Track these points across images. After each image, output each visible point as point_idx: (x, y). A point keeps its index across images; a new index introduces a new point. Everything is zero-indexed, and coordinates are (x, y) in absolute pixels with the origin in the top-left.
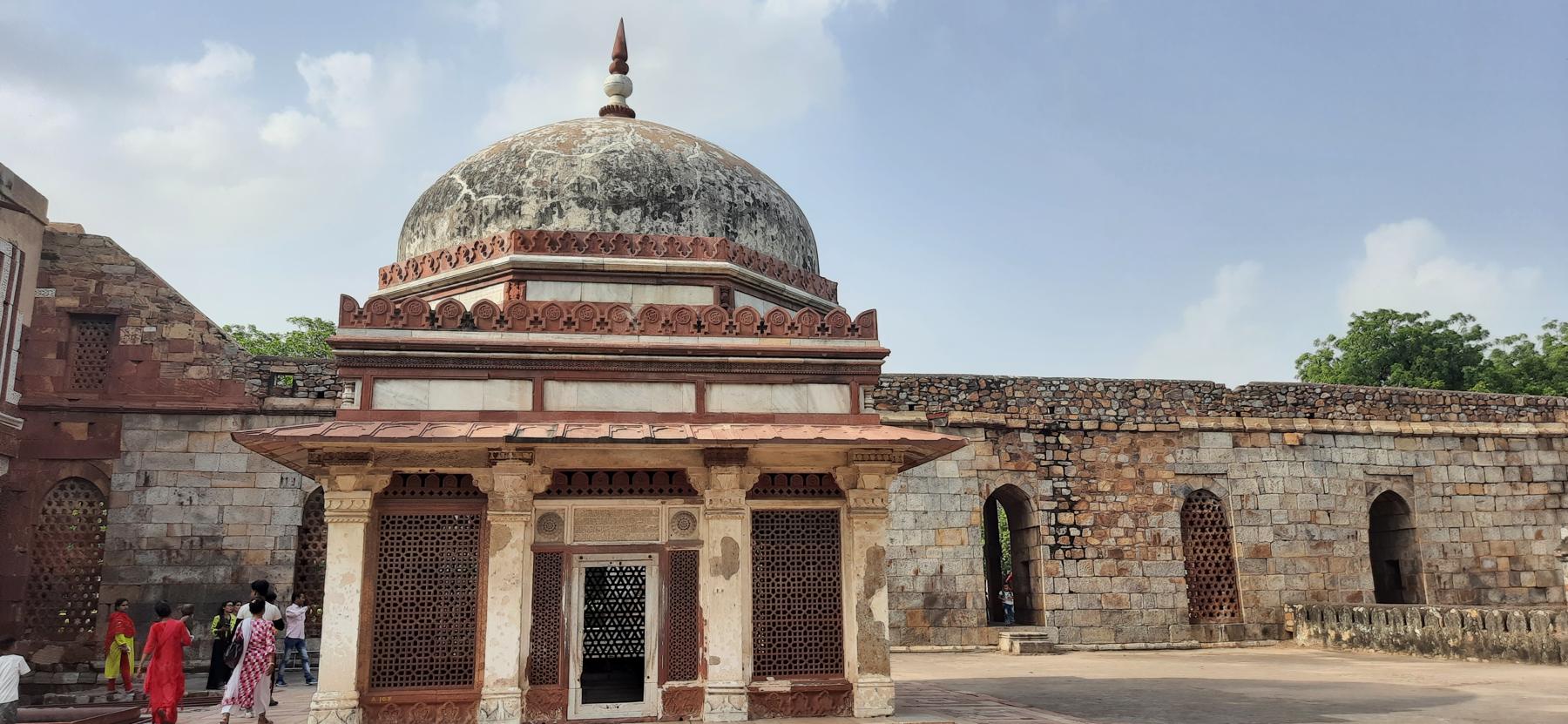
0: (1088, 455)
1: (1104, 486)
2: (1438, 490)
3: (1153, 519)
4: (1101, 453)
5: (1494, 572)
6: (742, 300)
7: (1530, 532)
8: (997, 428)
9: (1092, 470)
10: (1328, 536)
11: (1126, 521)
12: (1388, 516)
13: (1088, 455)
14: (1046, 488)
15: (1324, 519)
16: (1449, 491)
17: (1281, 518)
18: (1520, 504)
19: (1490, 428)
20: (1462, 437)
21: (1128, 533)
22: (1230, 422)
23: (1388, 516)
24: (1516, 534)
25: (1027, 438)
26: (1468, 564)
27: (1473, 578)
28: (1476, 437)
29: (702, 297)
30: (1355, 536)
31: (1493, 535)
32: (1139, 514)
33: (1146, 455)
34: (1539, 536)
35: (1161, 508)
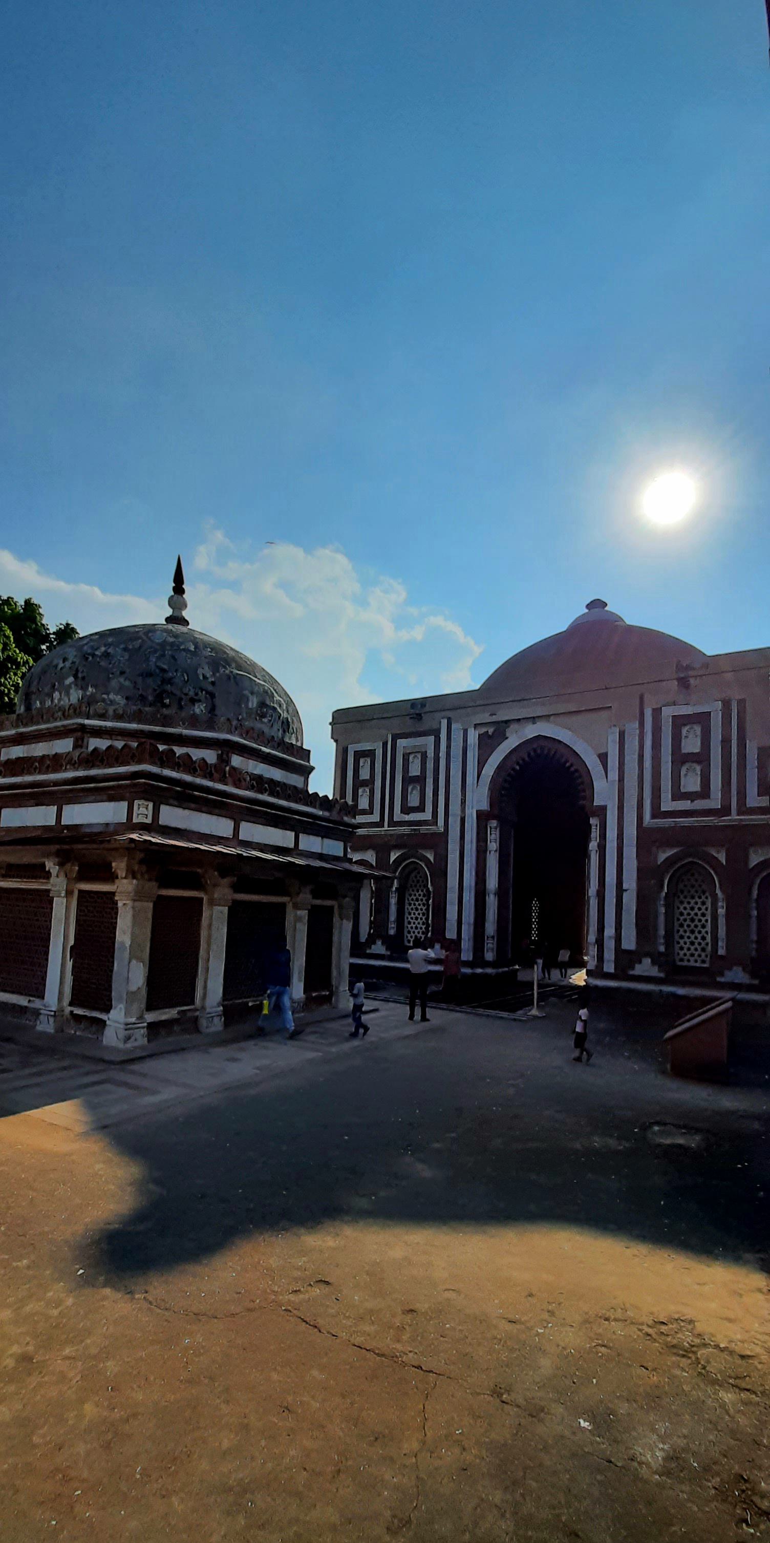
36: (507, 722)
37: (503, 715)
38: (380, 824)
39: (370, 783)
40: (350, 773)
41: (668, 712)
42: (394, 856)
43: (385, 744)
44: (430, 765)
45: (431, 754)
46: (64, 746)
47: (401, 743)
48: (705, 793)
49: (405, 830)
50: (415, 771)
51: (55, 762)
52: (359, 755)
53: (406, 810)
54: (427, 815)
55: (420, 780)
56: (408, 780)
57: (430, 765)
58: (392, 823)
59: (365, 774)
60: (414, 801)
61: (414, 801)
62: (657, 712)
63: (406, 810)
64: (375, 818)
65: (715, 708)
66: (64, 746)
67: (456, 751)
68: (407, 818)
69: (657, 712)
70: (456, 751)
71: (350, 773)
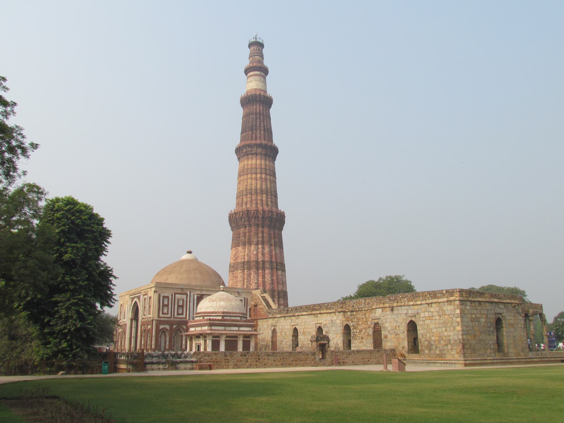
0: (358, 316)
1: (360, 323)
3: (368, 330)
4: (360, 315)
5: (434, 341)
6: (206, 318)
7: (444, 329)
8: (344, 312)
9: (358, 319)
10: (398, 332)
11: (364, 331)
12: (412, 327)
13: (358, 316)
14: (352, 324)
15: (398, 328)
16: (424, 319)
17: (389, 329)
18: (441, 321)
19: (436, 300)
20: (428, 304)
21: (364, 333)
22: (382, 306)
23: (412, 327)
24: (440, 330)
25: (349, 313)
26: (428, 338)
27: (429, 342)
28: (432, 303)
29: (202, 318)
30: (404, 332)
31: (434, 330)
32: (366, 329)
33: (367, 315)
34: (446, 330)
35: (369, 327)
36: (204, 295)
37: (203, 293)
38: (171, 317)
39: (167, 305)
42: (175, 326)
44: (185, 303)
45: (185, 300)
46: (239, 318)
49: (179, 319)
50: (181, 303)
51: (238, 321)
52: (164, 297)
53: (178, 314)
54: (184, 316)
55: (182, 306)
56: (179, 306)
57: (185, 303)
58: (174, 317)
59: (166, 303)
60: (180, 312)
61: (180, 312)
64: (169, 316)
66: (239, 318)
67: (192, 300)
70: (192, 300)
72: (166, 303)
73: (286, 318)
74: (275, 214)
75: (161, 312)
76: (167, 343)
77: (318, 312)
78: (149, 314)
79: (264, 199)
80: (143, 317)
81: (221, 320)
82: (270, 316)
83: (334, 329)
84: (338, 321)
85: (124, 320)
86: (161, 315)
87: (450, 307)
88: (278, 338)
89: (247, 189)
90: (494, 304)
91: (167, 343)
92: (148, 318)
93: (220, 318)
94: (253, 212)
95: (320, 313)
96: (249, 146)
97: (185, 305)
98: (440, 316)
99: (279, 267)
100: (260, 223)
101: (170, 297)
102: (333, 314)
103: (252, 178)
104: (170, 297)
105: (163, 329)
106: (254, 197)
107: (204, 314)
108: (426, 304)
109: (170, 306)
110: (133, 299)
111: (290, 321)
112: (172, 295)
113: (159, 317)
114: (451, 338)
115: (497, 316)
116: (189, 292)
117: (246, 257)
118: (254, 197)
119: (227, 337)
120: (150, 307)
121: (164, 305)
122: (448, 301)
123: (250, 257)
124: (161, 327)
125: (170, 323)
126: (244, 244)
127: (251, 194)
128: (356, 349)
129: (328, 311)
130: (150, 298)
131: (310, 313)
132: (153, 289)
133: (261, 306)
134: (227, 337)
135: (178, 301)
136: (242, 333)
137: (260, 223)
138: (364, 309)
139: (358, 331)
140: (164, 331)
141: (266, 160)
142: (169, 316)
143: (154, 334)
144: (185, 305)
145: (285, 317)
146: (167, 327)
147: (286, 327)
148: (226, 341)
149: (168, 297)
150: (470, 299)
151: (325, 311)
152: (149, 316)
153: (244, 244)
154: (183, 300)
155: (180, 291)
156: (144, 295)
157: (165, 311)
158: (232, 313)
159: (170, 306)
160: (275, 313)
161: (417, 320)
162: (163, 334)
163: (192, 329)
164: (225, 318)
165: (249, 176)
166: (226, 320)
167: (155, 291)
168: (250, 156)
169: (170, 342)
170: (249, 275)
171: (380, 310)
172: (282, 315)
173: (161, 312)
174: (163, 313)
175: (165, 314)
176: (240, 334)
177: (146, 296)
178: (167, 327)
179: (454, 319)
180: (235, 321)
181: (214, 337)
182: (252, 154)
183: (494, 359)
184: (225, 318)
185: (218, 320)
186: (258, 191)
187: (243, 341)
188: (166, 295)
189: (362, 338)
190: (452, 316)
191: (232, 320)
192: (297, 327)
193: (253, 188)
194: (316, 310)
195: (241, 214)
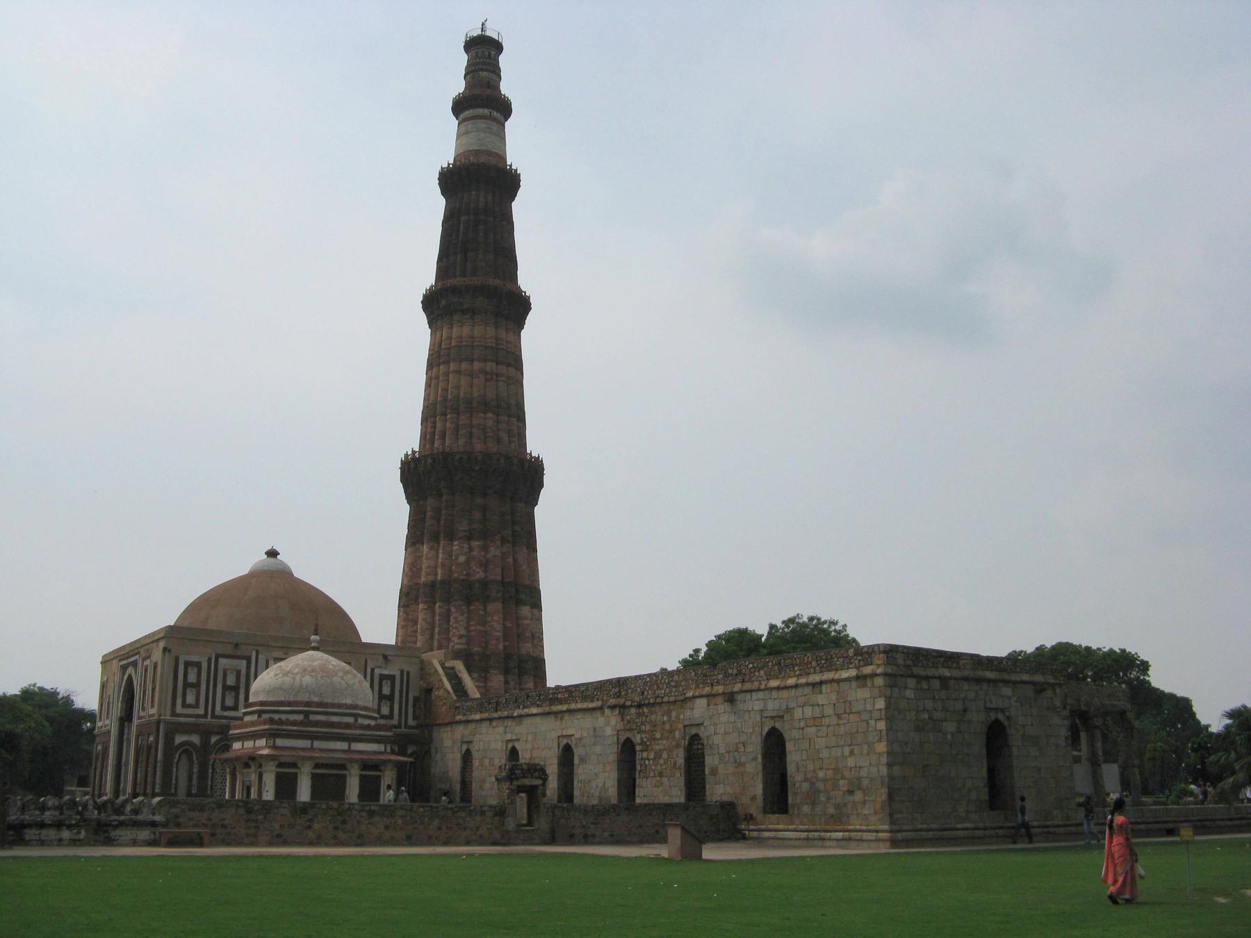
1: (658, 736)
2: (796, 724)
4: (658, 716)
5: (824, 780)
7: (847, 750)
8: (623, 707)
10: (743, 759)
11: (665, 755)
12: (774, 745)
13: (653, 717)
15: (742, 749)
16: (802, 724)
17: (722, 750)
18: (842, 730)
19: (828, 676)
20: (814, 685)
22: (707, 690)
23: (774, 745)
24: (837, 752)
25: (633, 710)
27: (812, 784)
28: (821, 683)
30: (755, 759)
31: (825, 754)
32: (670, 751)
33: (674, 714)
34: (852, 753)
35: (678, 746)
38: (205, 716)
39: (197, 686)
40: (181, 676)
41: (377, 671)
42: (214, 739)
43: (210, 660)
44: (243, 679)
45: (243, 672)
46: (351, 720)
47: (223, 661)
48: (391, 716)
50: (231, 681)
51: (347, 726)
52: (188, 664)
53: (224, 708)
55: (236, 689)
56: (226, 688)
57: (243, 679)
58: (213, 716)
59: (192, 678)
61: (229, 702)
62: (373, 670)
63: (224, 708)
64: (201, 711)
65: (397, 674)
68: (226, 714)
69: (373, 670)
71: (181, 676)
72: (192, 678)
73: (494, 724)
74: (515, 461)
75: (179, 701)
76: (195, 782)
77: (565, 707)
78: (152, 706)
79: (490, 423)
80: (142, 714)
81: (301, 723)
82: (458, 718)
83: (598, 749)
84: (609, 731)
85: (108, 722)
86: (179, 709)
87: (864, 693)
88: (475, 774)
89: (445, 399)
90: (985, 686)
91: (195, 782)
92: (150, 716)
93: (300, 717)
94: (457, 457)
95: (570, 711)
96: (454, 290)
97: (242, 685)
98: (839, 716)
99: (523, 596)
100: (474, 482)
101: (205, 665)
102: (598, 714)
103: (458, 372)
104: (205, 665)
105: (183, 744)
106: (464, 419)
107: (266, 708)
108: (807, 684)
109: (203, 687)
110: (124, 668)
111: (501, 729)
112: (210, 660)
113: (174, 714)
114: (864, 773)
115: (993, 716)
116: (254, 654)
117: (439, 571)
118: (464, 419)
119: (317, 766)
120: (153, 689)
121: (187, 685)
122: (857, 678)
123: (450, 570)
124: (179, 739)
125: (205, 733)
126: (435, 538)
127: (457, 411)
128: (645, 801)
129: (585, 705)
130: (155, 667)
131: (547, 709)
132: (162, 644)
133: (441, 693)
134: (317, 766)
135: (225, 676)
136: (357, 756)
137: (474, 482)
138: (666, 699)
139: (652, 756)
140: (187, 749)
141: (497, 327)
142: (201, 711)
143: (160, 757)
144: (242, 685)
145: (491, 720)
146: (195, 739)
147: (493, 746)
148: (315, 777)
149: (198, 665)
150: (916, 670)
151: (579, 706)
152: (153, 711)
153: (435, 538)
154: (238, 673)
155: (229, 650)
156: (144, 659)
157: (190, 699)
158: (333, 705)
159: (203, 687)
160: (470, 710)
161: (787, 726)
162: (184, 757)
163: (237, 746)
164: (312, 717)
165: (453, 366)
166: (317, 724)
167: (165, 650)
168: (456, 317)
169: (203, 776)
170: (446, 617)
171: (704, 701)
172: (485, 715)
173: (179, 701)
174: (184, 705)
175: (190, 706)
176: (352, 761)
177: (147, 662)
178: (195, 739)
179: (872, 722)
180: (339, 725)
181: (281, 765)
182: (464, 312)
183: (928, 830)
184: (312, 717)
185: (294, 723)
186: (475, 405)
187: (362, 778)
188: (195, 659)
189: (661, 774)
190: (865, 716)
191: (332, 725)
192: (517, 745)
193: (462, 395)
194: (560, 702)
195: (429, 461)
